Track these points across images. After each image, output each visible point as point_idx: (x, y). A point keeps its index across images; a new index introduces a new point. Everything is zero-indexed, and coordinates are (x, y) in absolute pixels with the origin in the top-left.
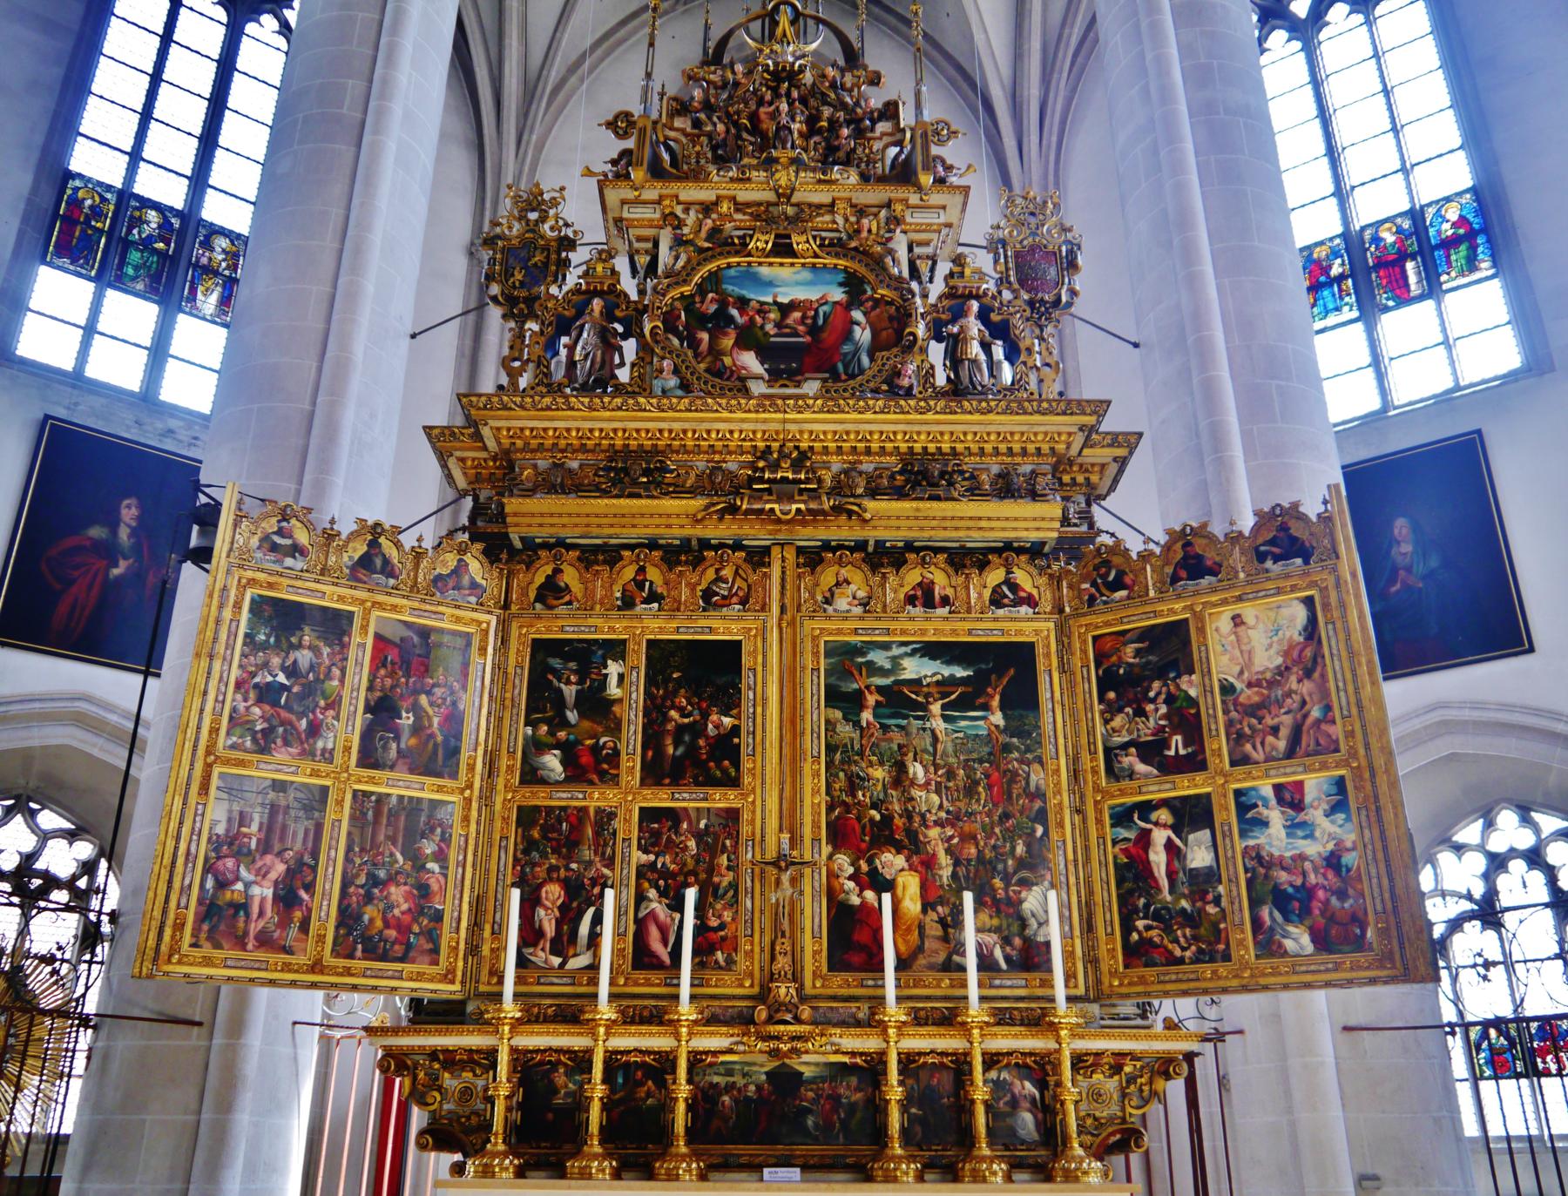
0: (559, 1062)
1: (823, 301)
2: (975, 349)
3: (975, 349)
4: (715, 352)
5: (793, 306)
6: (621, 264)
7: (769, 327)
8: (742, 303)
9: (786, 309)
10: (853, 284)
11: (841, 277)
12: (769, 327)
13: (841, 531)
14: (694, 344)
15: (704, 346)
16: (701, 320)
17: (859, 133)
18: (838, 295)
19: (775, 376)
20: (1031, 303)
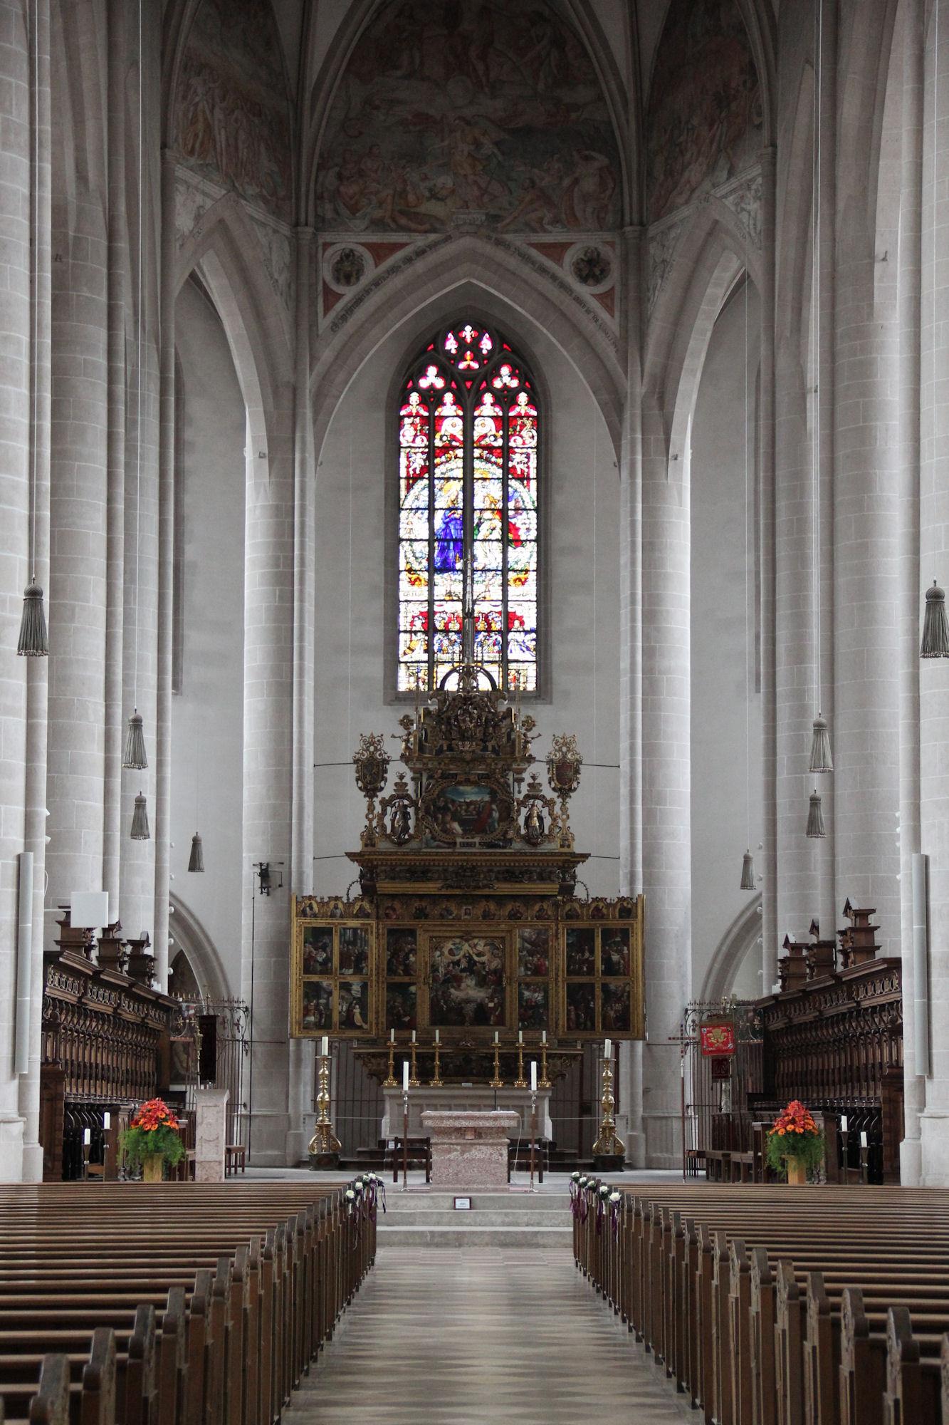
1: (482, 801)
2: (536, 822)
3: (536, 822)
4: (444, 823)
5: (471, 803)
6: (407, 780)
7: (463, 813)
8: (453, 802)
9: (468, 804)
10: (493, 793)
11: (488, 790)
12: (463, 813)
13: (486, 892)
14: (436, 819)
15: (440, 821)
16: (438, 809)
17: (496, 726)
18: (487, 798)
19: (466, 832)
20: (560, 789)
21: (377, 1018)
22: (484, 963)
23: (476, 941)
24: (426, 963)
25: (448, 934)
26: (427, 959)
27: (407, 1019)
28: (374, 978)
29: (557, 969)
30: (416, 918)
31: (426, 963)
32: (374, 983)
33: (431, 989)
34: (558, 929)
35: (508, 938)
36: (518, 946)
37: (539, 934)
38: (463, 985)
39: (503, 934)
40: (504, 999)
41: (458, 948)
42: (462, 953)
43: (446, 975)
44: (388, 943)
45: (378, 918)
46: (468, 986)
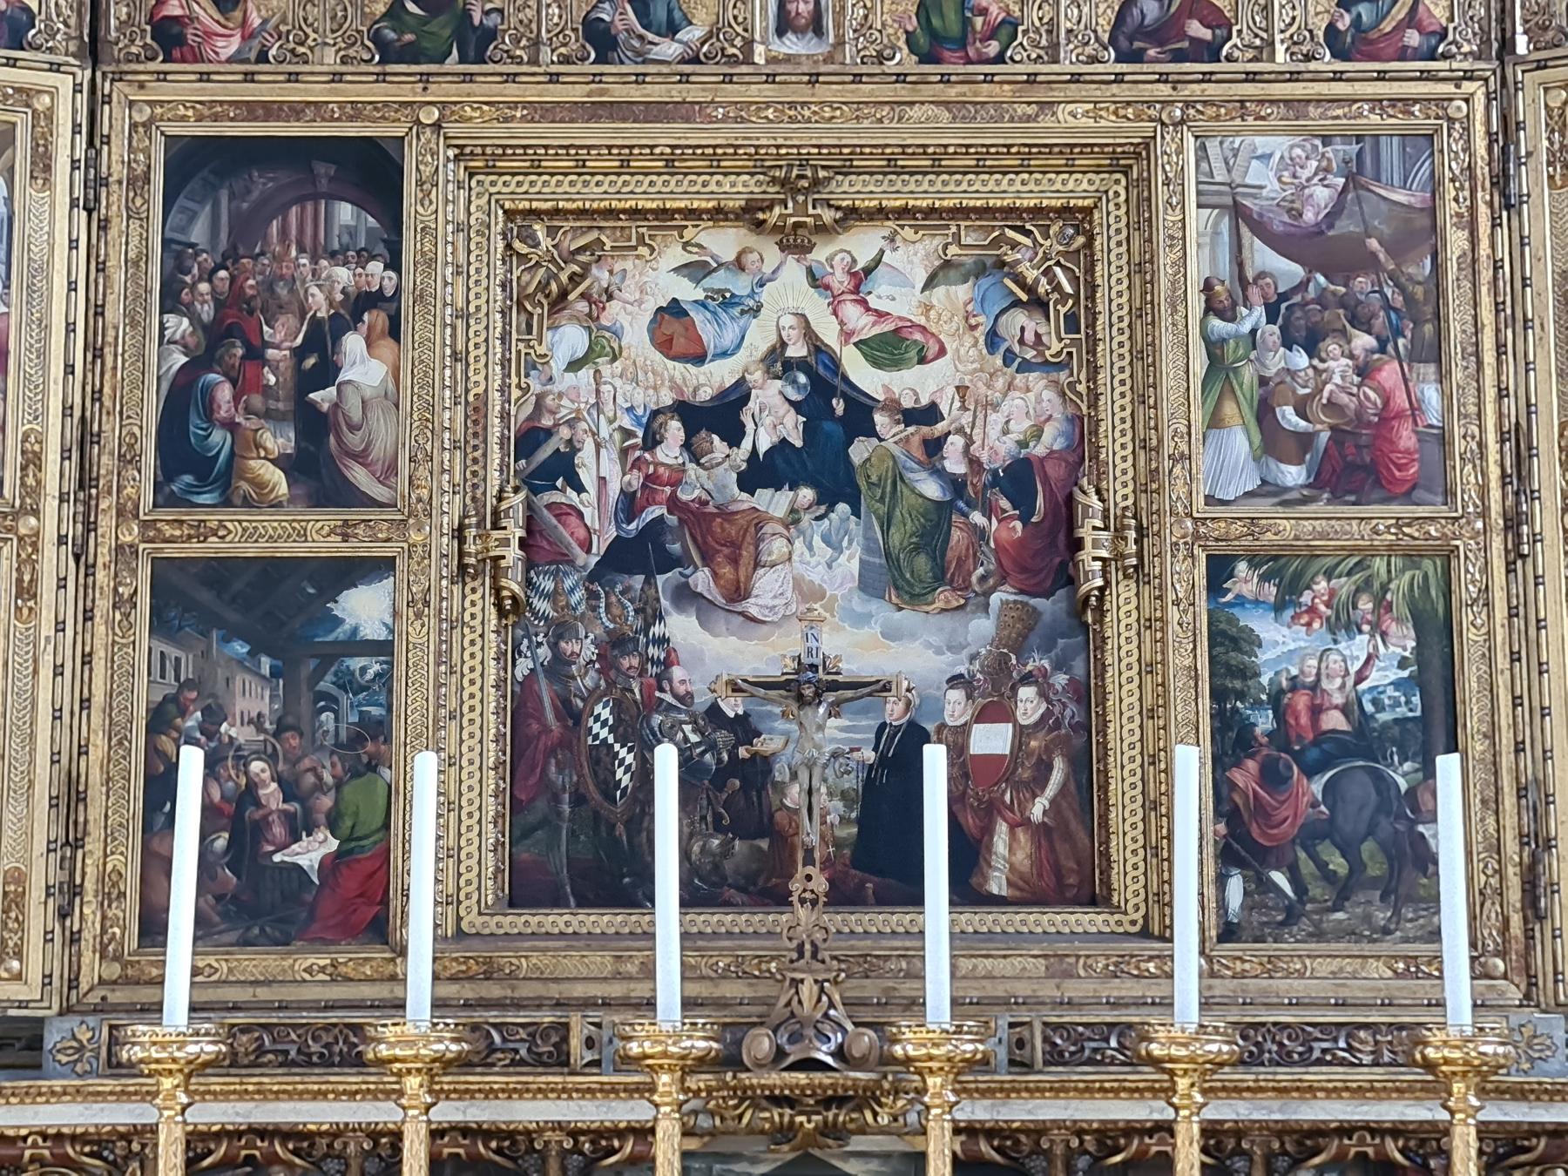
0: (274, 1159)
21: (73, 841)
22: (930, 414)
23: (863, 243)
24: (477, 412)
25: (646, 192)
26: (487, 378)
27: (311, 852)
28: (52, 519)
29: (1519, 441)
30: (389, 53)
31: (477, 412)
32: (51, 560)
33: (511, 610)
34: (1509, 127)
35: (1111, 221)
36: (1196, 273)
37: (1356, 176)
38: (768, 588)
39: (1077, 188)
40: (1088, 694)
41: (728, 301)
42: (759, 338)
43: (630, 505)
44: (177, 254)
45: (93, 50)
46: (808, 593)
